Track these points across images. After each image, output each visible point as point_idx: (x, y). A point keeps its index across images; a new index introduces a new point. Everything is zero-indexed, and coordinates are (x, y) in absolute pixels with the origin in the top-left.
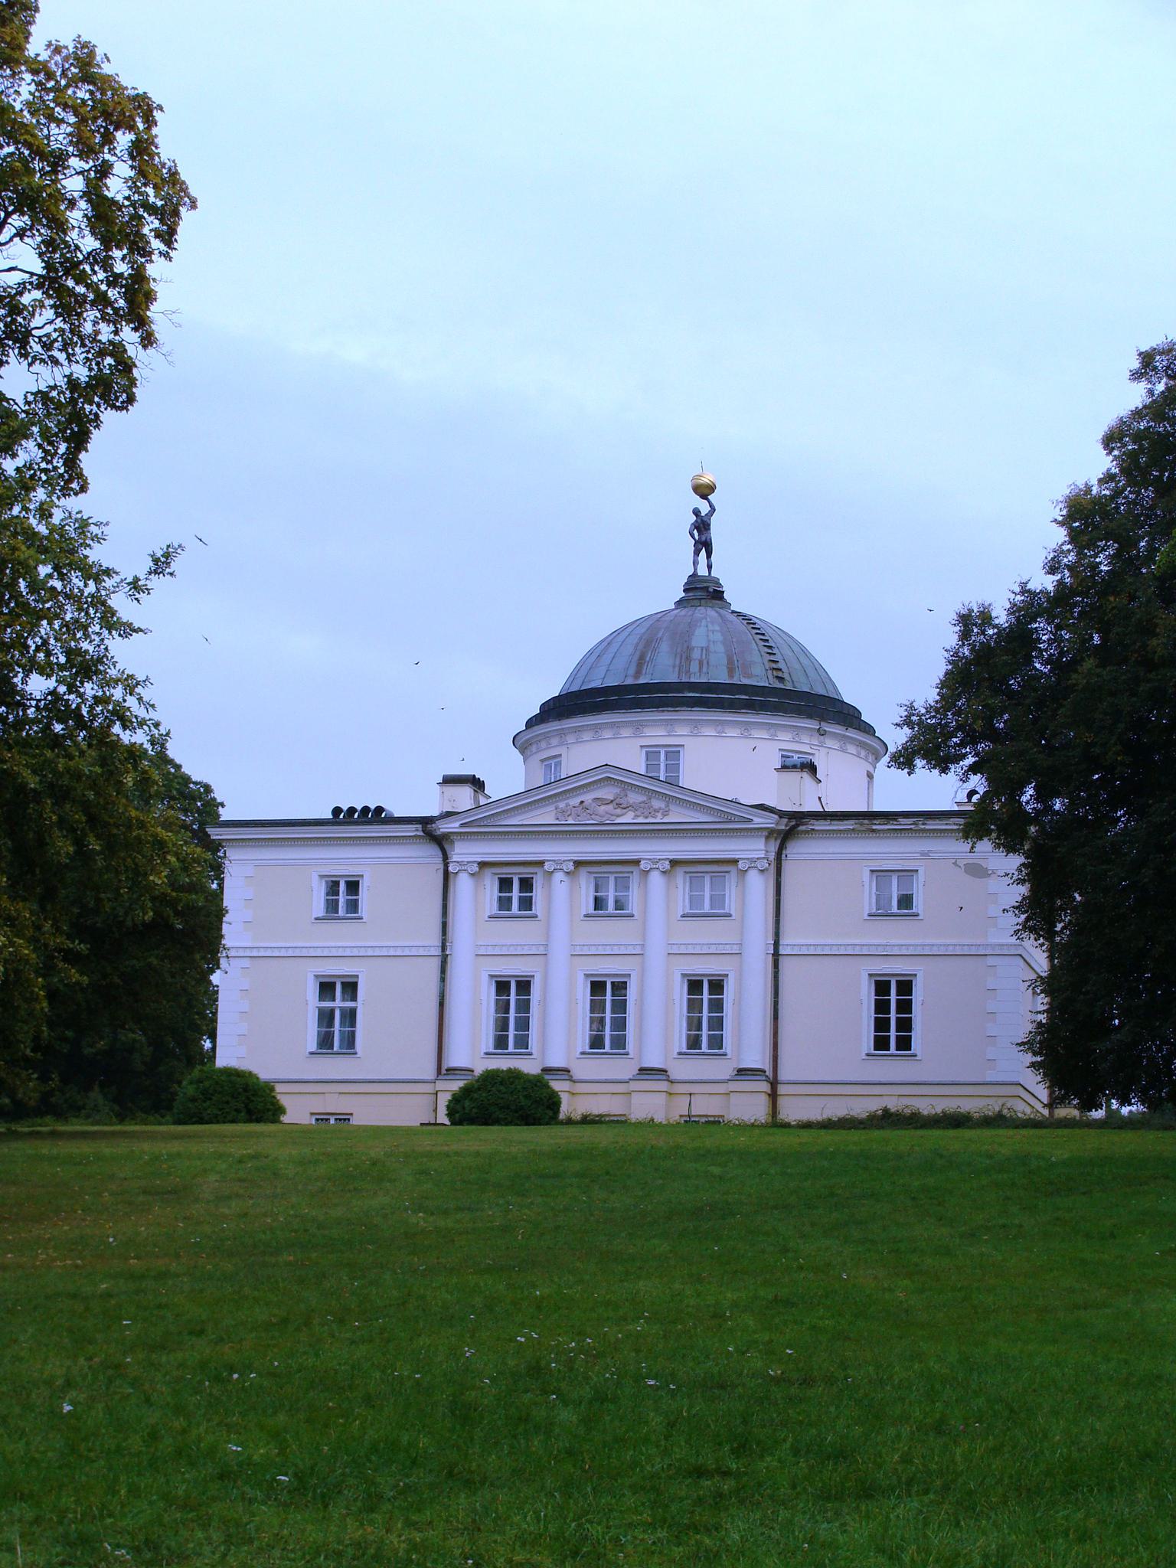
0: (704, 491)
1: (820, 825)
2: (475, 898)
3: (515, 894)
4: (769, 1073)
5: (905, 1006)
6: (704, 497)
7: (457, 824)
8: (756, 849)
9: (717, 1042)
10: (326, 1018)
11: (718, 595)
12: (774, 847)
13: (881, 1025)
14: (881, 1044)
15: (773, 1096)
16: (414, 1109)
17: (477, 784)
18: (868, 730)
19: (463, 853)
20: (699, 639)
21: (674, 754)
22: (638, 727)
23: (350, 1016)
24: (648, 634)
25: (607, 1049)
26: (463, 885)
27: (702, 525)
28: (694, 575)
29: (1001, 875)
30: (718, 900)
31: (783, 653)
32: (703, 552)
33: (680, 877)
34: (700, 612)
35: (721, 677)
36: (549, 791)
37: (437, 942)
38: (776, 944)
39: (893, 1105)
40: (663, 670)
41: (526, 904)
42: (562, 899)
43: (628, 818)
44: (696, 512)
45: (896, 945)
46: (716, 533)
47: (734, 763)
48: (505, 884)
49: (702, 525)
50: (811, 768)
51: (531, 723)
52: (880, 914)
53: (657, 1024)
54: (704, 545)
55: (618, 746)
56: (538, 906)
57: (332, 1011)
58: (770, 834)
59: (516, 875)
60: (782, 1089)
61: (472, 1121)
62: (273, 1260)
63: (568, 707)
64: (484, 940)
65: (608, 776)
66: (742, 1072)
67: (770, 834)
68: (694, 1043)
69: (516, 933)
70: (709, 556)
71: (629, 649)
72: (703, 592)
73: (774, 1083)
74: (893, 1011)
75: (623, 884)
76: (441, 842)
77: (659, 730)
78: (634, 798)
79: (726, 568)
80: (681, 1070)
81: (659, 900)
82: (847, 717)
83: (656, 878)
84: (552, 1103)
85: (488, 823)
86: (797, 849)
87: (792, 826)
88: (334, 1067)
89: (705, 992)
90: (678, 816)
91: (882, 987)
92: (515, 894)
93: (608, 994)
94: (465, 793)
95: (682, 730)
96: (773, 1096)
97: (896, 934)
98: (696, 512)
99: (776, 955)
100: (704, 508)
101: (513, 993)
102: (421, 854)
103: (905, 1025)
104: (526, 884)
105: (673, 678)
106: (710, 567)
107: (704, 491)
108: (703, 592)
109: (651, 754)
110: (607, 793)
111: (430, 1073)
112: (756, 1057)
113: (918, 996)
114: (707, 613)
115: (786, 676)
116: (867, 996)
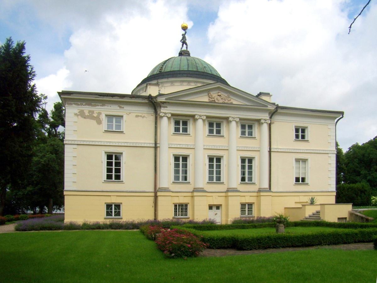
2: (167, 126)
7: (164, 98)
8: (266, 116)
25: (215, 181)
37: (153, 142)
38: (270, 149)
41: (185, 130)
48: (177, 123)
64: (171, 142)
69: (182, 140)
88: (113, 186)
89: (247, 163)
93: (215, 162)
97: (301, 146)
99: (270, 152)
101: (181, 161)
102: (146, 110)
106: (187, 48)
111: (152, 189)
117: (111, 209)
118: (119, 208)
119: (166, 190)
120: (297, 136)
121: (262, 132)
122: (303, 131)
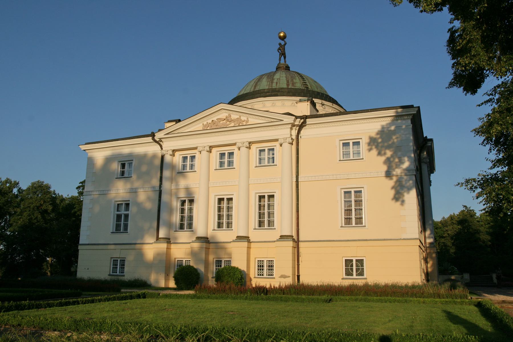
4: (295, 237)
6: (283, 40)
7: (163, 135)
10: (119, 217)
11: (287, 68)
12: (294, 132)
14: (348, 221)
23: (127, 216)
32: (283, 57)
43: (232, 125)
44: (280, 44)
54: (283, 54)
57: (121, 215)
60: (301, 244)
66: (282, 237)
70: (285, 58)
73: (297, 242)
88: (121, 238)
89: (266, 202)
98: (280, 44)
100: (283, 43)
106: (285, 62)
113: (365, 197)
115: (309, 87)
117: (352, 266)
118: (362, 265)
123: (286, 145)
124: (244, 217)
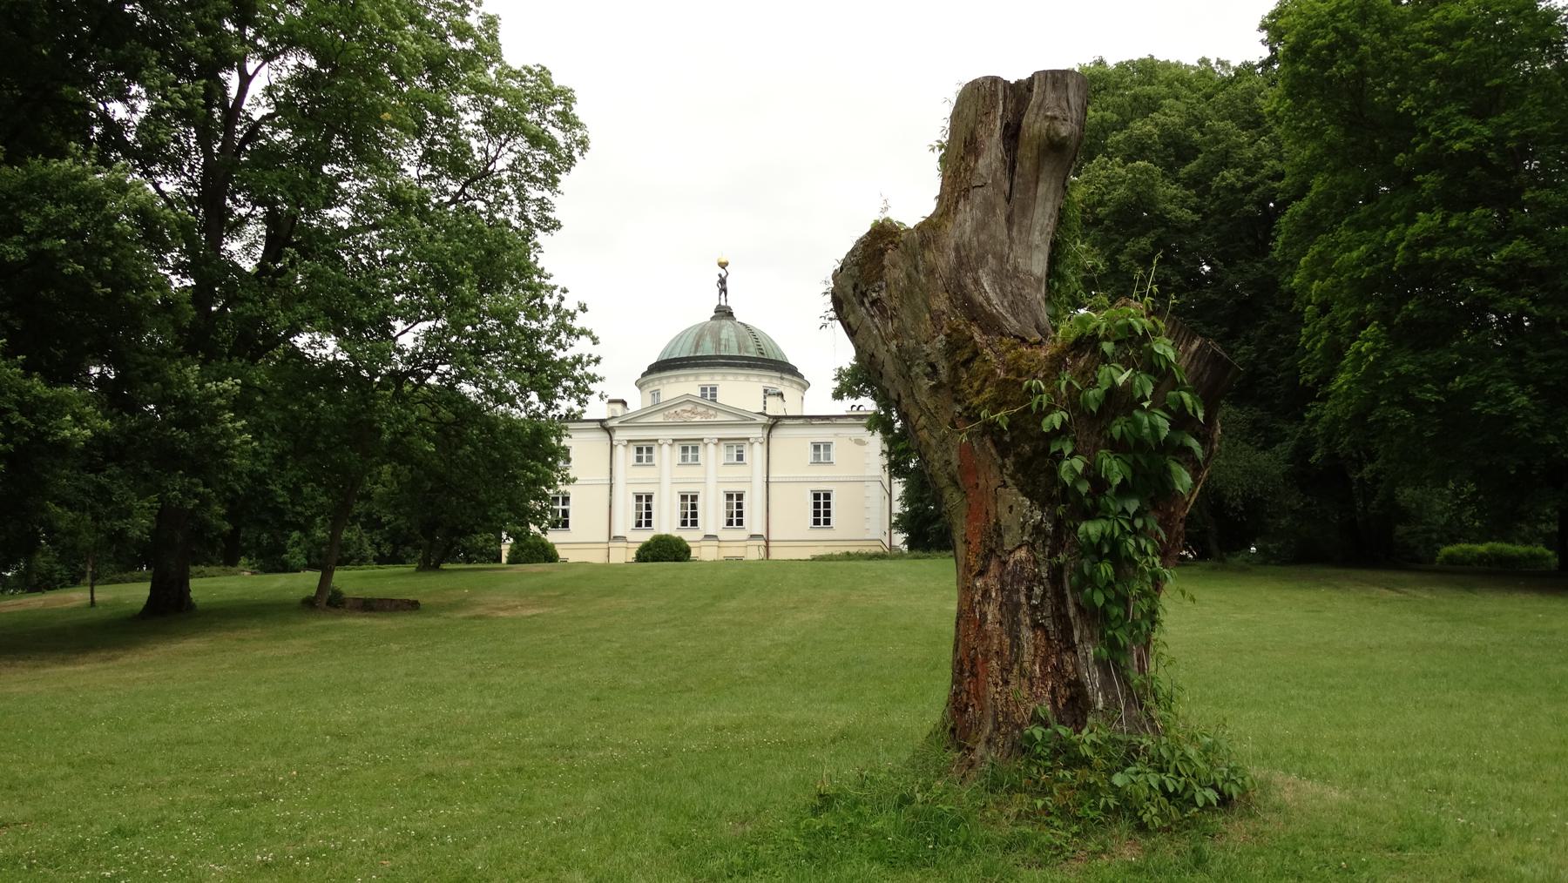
0: (723, 265)
1: (787, 422)
2: (626, 457)
3: (644, 454)
5: (827, 505)
8: (758, 433)
9: (740, 523)
11: (730, 314)
13: (817, 514)
14: (817, 522)
15: (767, 547)
16: (623, 555)
17: (624, 403)
18: (801, 377)
19: (620, 436)
20: (724, 335)
21: (714, 389)
22: (697, 376)
24: (700, 333)
26: (619, 451)
27: (723, 281)
28: (719, 306)
29: (875, 443)
30: (740, 458)
31: (762, 341)
33: (722, 446)
34: (724, 322)
35: (736, 353)
36: (657, 407)
39: (853, 550)
40: (708, 349)
41: (650, 459)
42: (667, 457)
43: (698, 419)
45: (822, 477)
46: (729, 285)
47: (742, 392)
48: (639, 450)
49: (723, 281)
50: (781, 395)
51: (644, 375)
52: (817, 461)
53: (712, 514)
54: (724, 290)
55: (684, 386)
56: (656, 460)
58: (764, 426)
59: (690, 445)
61: (646, 560)
62: (1072, 612)
63: (662, 366)
65: (687, 400)
67: (764, 426)
68: (730, 523)
69: (644, 473)
71: (690, 340)
72: (724, 313)
73: (767, 541)
74: (822, 508)
75: (695, 449)
76: (609, 431)
77: (707, 378)
78: (700, 409)
79: (733, 302)
80: (723, 535)
81: (713, 457)
82: (792, 371)
83: (711, 446)
84: (688, 551)
85: (629, 423)
86: (776, 433)
87: (775, 422)
89: (735, 500)
90: (721, 417)
91: (817, 496)
92: (644, 454)
94: (619, 407)
95: (718, 378)
96: (767, 547)
97: (822, 472)
101: (645, 503)
103: (827, 513)
104: (649, 450)
105: (712, 353)
107: (723, 265)
108: (724, 313)
109: (704, 389)
110: (688, 407)
112: (759, 529)
113: (833, 501)
114: (726, 323)
116: (810, 501)
119: (623, 538)
120: (817, 457)
121: (755, 454)
122: (828, 446)
123: (757, 446)
124: (712, 514)
